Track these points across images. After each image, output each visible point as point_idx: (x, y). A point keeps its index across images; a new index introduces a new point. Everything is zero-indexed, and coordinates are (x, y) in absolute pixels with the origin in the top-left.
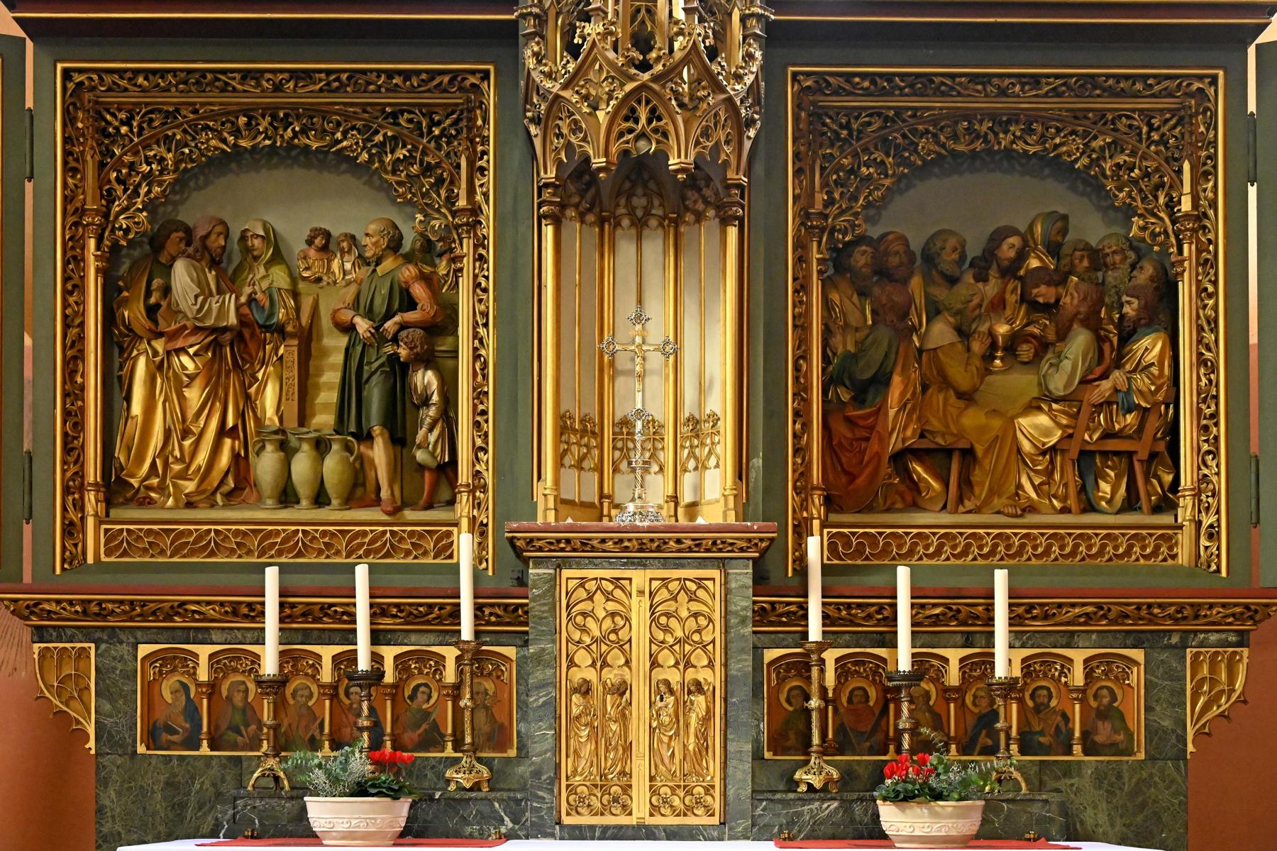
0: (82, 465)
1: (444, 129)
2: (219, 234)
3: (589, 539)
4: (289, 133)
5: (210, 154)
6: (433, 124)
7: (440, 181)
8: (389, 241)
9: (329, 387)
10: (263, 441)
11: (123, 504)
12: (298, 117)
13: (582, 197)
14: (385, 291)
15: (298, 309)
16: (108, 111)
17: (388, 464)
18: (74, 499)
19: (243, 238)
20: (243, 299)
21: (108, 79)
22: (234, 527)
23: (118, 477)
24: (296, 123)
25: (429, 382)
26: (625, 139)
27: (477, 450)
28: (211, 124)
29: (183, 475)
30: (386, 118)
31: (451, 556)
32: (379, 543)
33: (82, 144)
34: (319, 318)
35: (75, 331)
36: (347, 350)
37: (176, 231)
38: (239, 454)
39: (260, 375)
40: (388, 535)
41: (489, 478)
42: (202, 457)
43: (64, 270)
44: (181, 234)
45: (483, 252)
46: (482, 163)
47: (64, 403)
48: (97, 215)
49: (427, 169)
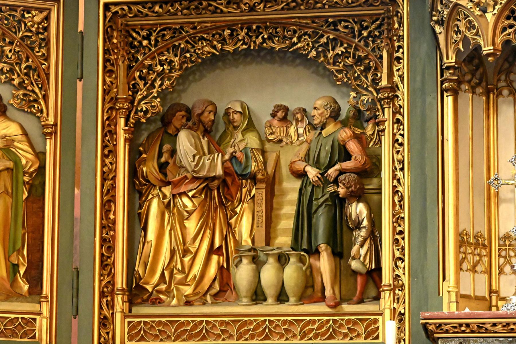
0: (113, 277)
1: (370, 32)
2: (210, 112)
3: (484, 324)
4: (260, 39)
5: (204, 57)
6: (363, 28)
7: (368, 69)
8: (331, 112)
9: (288, 217)
10: (241, 257)
11: (140, 303)
12: (266, 28)
13: (473, 75)
14: (328, 148)
15: (265, 163)
16: (134, 30)
17: (331, 270)
18: (107, 301)
19: (227, 113)
20: (227, 157)
21: (134, 8)
22: (219, 319)
23: (138, 285)
24: (264, 33)
25: (360, 212)
26: (507, 32)
27: (396, 260)
28: (205, 36)
29: (183, 282)
30: (329, 26)
31: (377, 338)
32: (324, 329)
33: (116, 54)
34: (280, 168)
35: (110, 182)
36: (301, 190)
37: (180, 111)
38: (223, 266)
39: (238, 210)
40: (331, 323)
41: (405, 280)
42: (197, 269)
43: (103, 141)
44: (183, 113)
45: (400, 117)
46: (399, 54)
47: (101, 233)
48: (126, 102)
49: (359, 61)
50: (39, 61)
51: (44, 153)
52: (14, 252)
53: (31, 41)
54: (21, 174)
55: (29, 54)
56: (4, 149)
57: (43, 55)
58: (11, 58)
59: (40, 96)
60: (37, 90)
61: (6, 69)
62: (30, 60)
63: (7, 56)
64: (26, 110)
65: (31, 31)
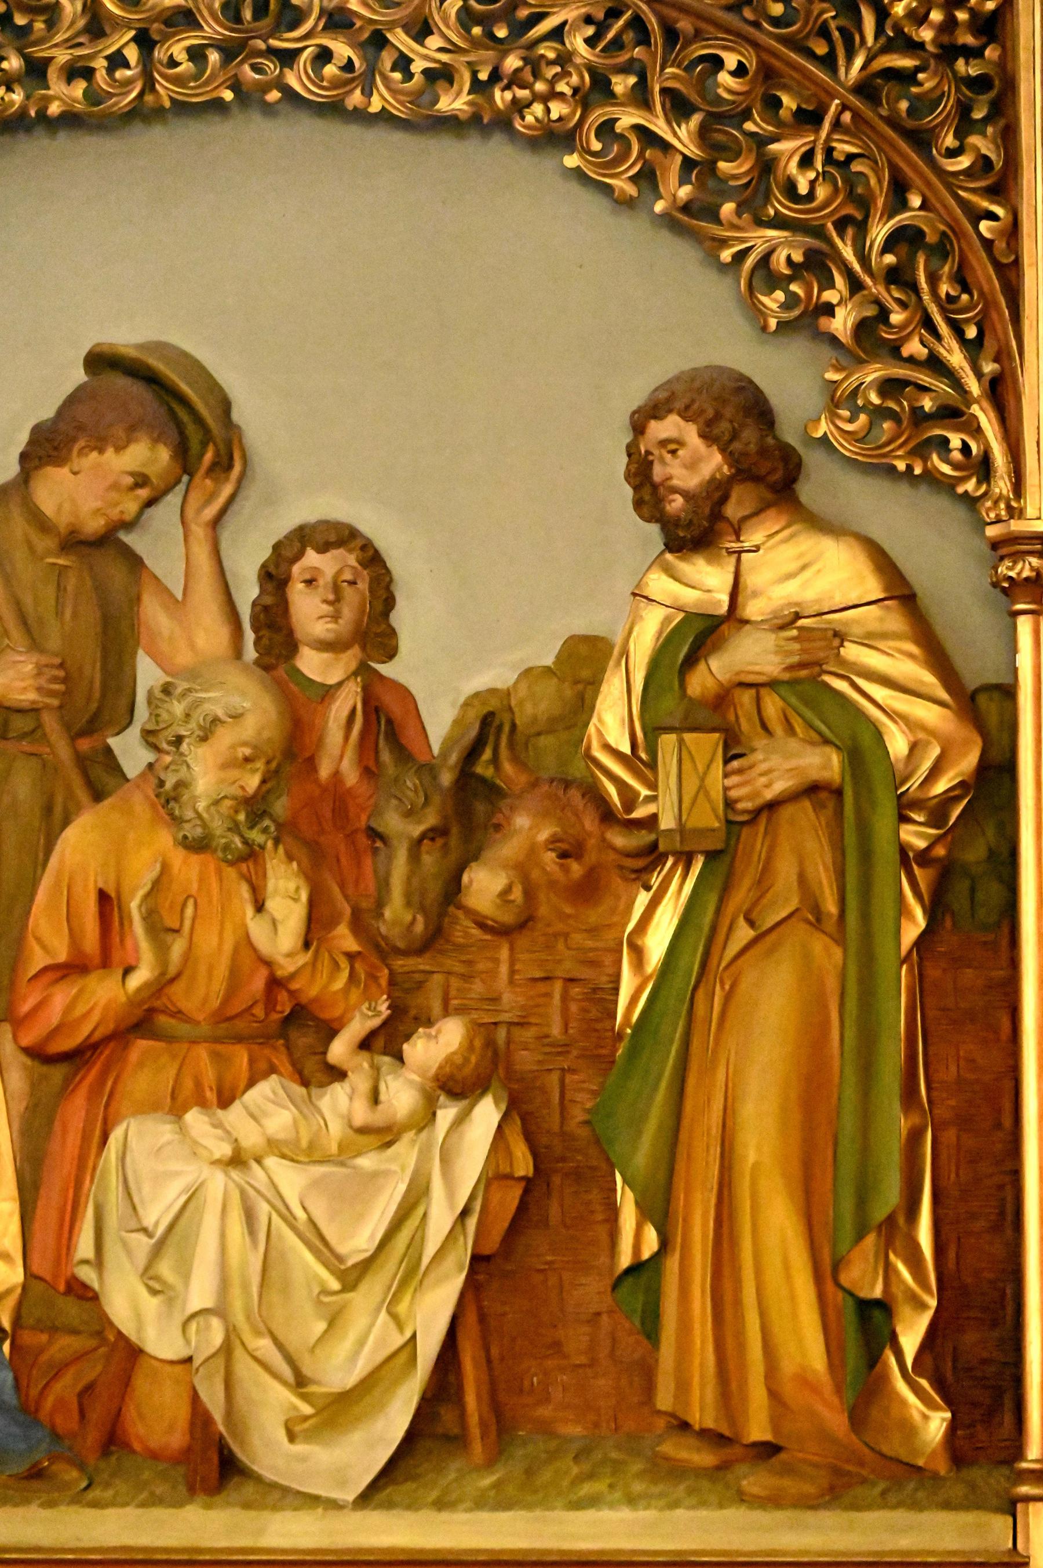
50: (962, 203)
51: (1008, 692)
52: (860, 1237)
53: (914, 100)
54: (887, 810)
55: (902, 165)
56: (792, 683)
57: (984, 164)
58: (811, 196)
59: (974, 387)
60: (956, 358)
61: (789, 258)
62: (916, 201)
63: (790, 188)
64: (901, 466)
65: (915, 47)
